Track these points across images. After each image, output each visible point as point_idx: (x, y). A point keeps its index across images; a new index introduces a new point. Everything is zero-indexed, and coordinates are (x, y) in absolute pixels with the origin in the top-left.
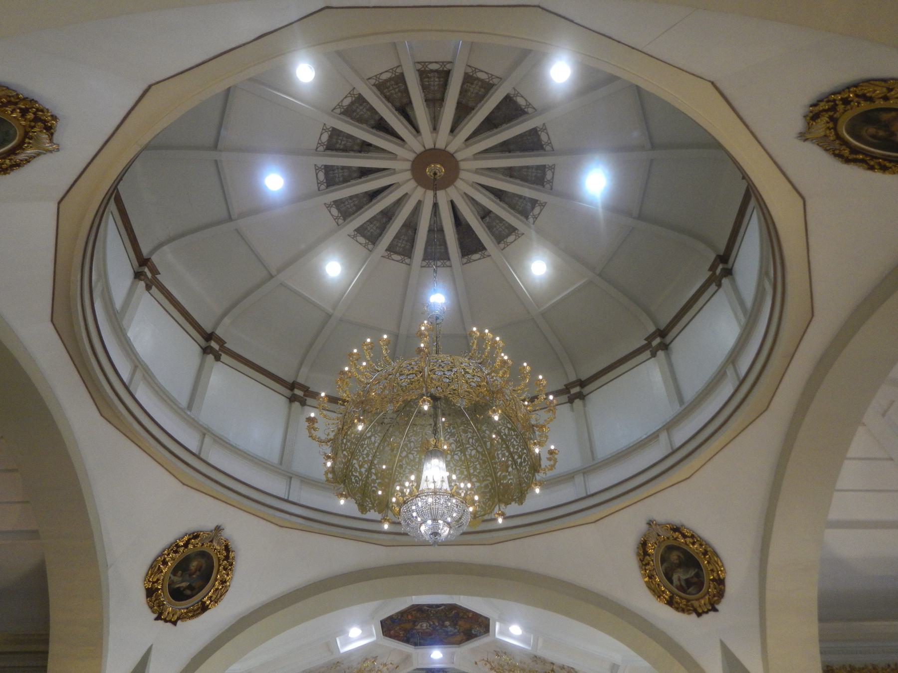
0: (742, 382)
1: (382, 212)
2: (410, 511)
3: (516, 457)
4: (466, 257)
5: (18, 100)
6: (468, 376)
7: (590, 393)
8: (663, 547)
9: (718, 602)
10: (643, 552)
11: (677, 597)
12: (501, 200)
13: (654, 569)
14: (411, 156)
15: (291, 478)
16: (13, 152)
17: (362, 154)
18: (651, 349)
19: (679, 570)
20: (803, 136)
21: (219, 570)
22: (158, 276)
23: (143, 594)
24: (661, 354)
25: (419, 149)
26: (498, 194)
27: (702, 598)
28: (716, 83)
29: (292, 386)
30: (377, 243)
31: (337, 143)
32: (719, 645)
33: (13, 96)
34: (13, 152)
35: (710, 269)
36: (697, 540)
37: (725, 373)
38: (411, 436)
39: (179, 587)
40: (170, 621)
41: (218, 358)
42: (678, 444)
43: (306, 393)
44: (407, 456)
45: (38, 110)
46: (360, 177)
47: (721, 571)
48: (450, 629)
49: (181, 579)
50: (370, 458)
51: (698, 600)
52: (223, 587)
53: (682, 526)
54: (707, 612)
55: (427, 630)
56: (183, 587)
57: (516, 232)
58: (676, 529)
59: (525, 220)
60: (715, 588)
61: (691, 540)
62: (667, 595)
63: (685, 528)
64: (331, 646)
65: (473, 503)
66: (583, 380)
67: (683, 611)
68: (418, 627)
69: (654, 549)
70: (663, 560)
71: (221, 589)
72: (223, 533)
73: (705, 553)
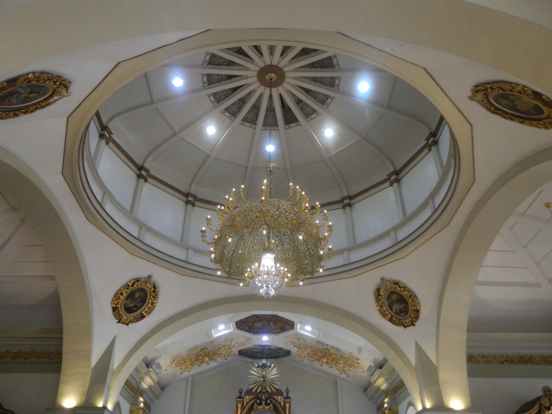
0: (436, 210)
1: (240, 99)
2: (254, 282)
3: (311, 251)
4: (288, 125)
5: (53, 78)
6: (287, 214)
7: (355, 203)
8: (388, 292)
9: (416, 321)
10: (378, 294)
11: (394, 318)
13: (383, 303)
14: (258, 69)
15: (188, 249)
16: (47, 99)
17: (229, 67)
18: (390, 181)
20: (471, 98)
21: (150, 297)
22: (112, 136)
23: (110, 310)
25: (262, 65)
26: (307, 91)
27: (407, 319)
29: (187, 195)
30: (236, 116)
31: (214, 61)
32: (414, 343)
33: (50, 77)
34: (47, 99)
35: (426, 140)
36: (407, 290)
37: (428, 203)
38: (255, 236)
39: (130, 307)
40: (125, 323)
41: (146, 180)
42: (400, 239)
43: (195, 199)
44: (253, 247)
45: (62, 80)
46: (227, 80)
47: (418, 306)
48: (273, 326)
49: (130, 302)
50: (233, 249)
51: (405, 319)
52: (152, 306)
53: (399, 282)
54: (409, 326)
55: (260, 327)
57: (317, 112)
58: (396, 283)
59: (322, 106)
60: (415, 314)
61: (404, 289)
62: (389, 316)
63: (401, 283)
64: (209, 334)
65: (287, 277)
66: (351, 196)
67: (397, 325)
68: (256, 325)
69: (383, 293)
70: (388, 298)
71: (151, 307)
72: (152, 279)
73: (410, 296)
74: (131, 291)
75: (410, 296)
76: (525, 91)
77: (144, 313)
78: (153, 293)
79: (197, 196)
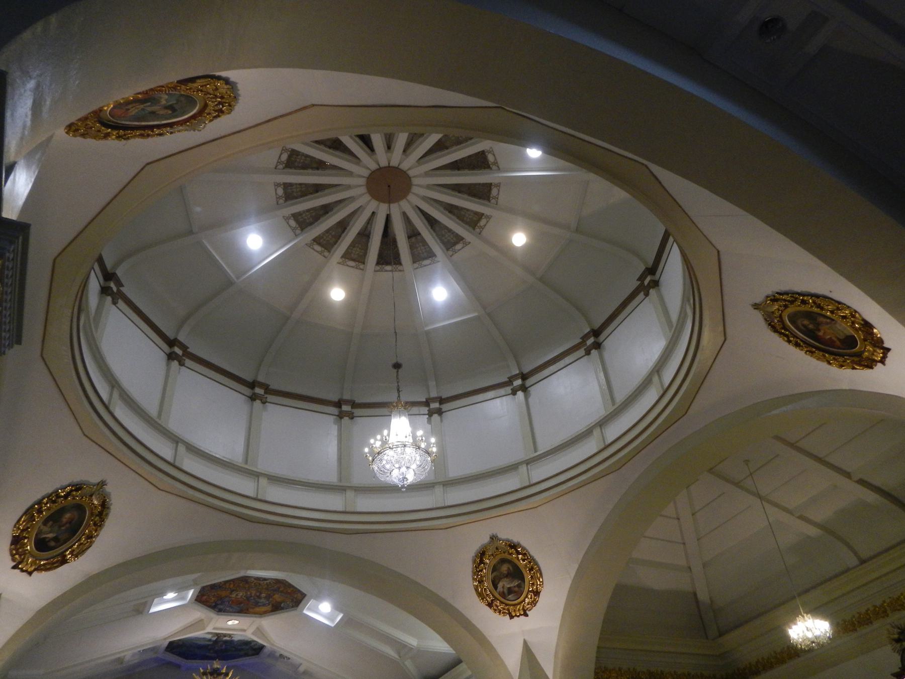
7: (449, 410)
8: (499, 557)
12: (432, 228)
15: (177, 443)
19: (505, 579)
24: (520, 394)
26: (432, 222)
28: (721, 253)
29: (171, 343)
39: (45, 538)
40: (26, 571)
48: (263, 600)
54: (518, 616)
56: (48, 537)
68: (234, 596)
70: (494, 569)
74: (59, 507)
75: (531, 569)
76: (853, 316)
77: (69, 554)
78: (97, 516)
79: (188, 348)
